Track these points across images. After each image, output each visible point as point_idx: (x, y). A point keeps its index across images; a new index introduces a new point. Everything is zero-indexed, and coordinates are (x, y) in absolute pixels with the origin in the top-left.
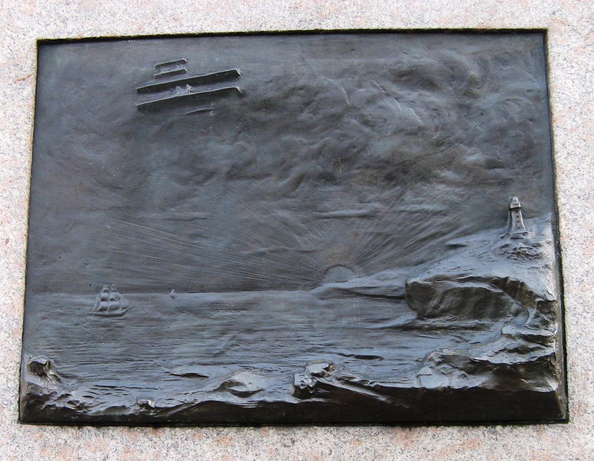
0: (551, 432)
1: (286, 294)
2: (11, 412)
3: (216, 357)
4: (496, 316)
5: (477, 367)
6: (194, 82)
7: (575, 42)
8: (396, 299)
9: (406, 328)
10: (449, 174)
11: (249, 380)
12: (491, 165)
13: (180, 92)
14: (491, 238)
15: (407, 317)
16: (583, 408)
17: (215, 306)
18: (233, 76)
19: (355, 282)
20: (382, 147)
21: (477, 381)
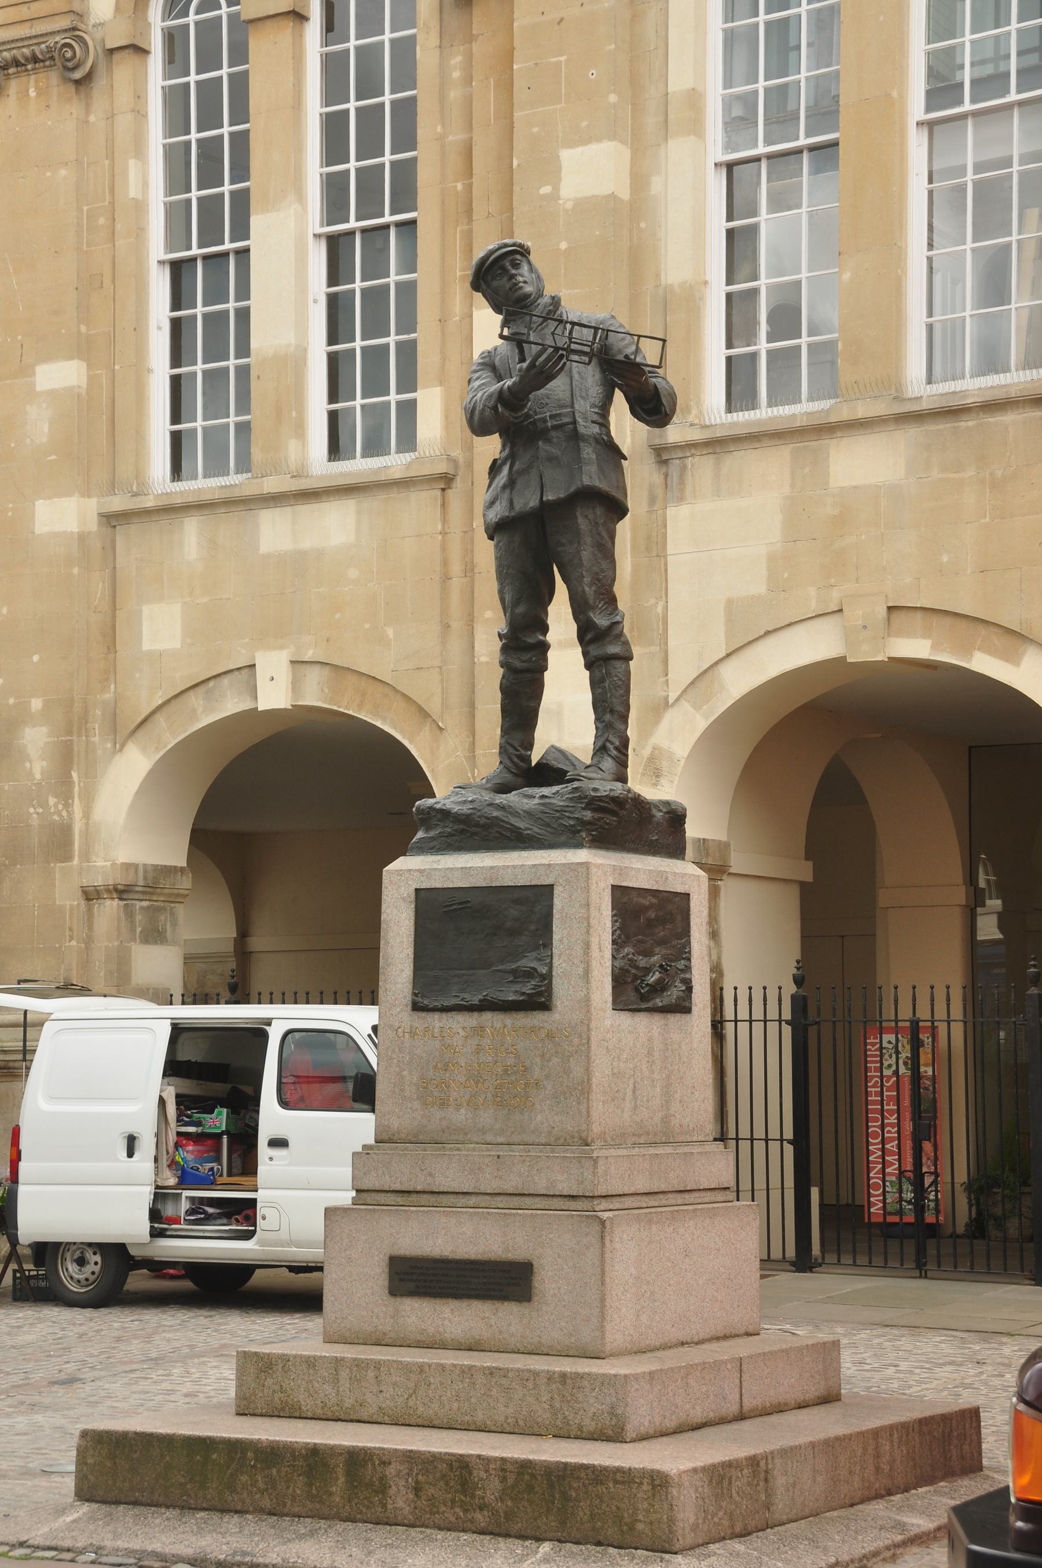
0: (547, 1013)
1: (483, 971)
2: (410, 1007)
3: (463, 991)
4: (532, 978)
5: (523, 994)
6: (459, 904)
7: (561, 889)
8: (510, 973)
9: (511, 982)
10: (526, 933)
11: (467, 996)
12: (537, 930)
13: (455, 907)
14: (534, 954)
15: (511, 979)
16: (556, 1006)
17: (464, 975)
18: (468, 902)
19: (501, 967)
20: (509, 924)
21: (521, 998)
